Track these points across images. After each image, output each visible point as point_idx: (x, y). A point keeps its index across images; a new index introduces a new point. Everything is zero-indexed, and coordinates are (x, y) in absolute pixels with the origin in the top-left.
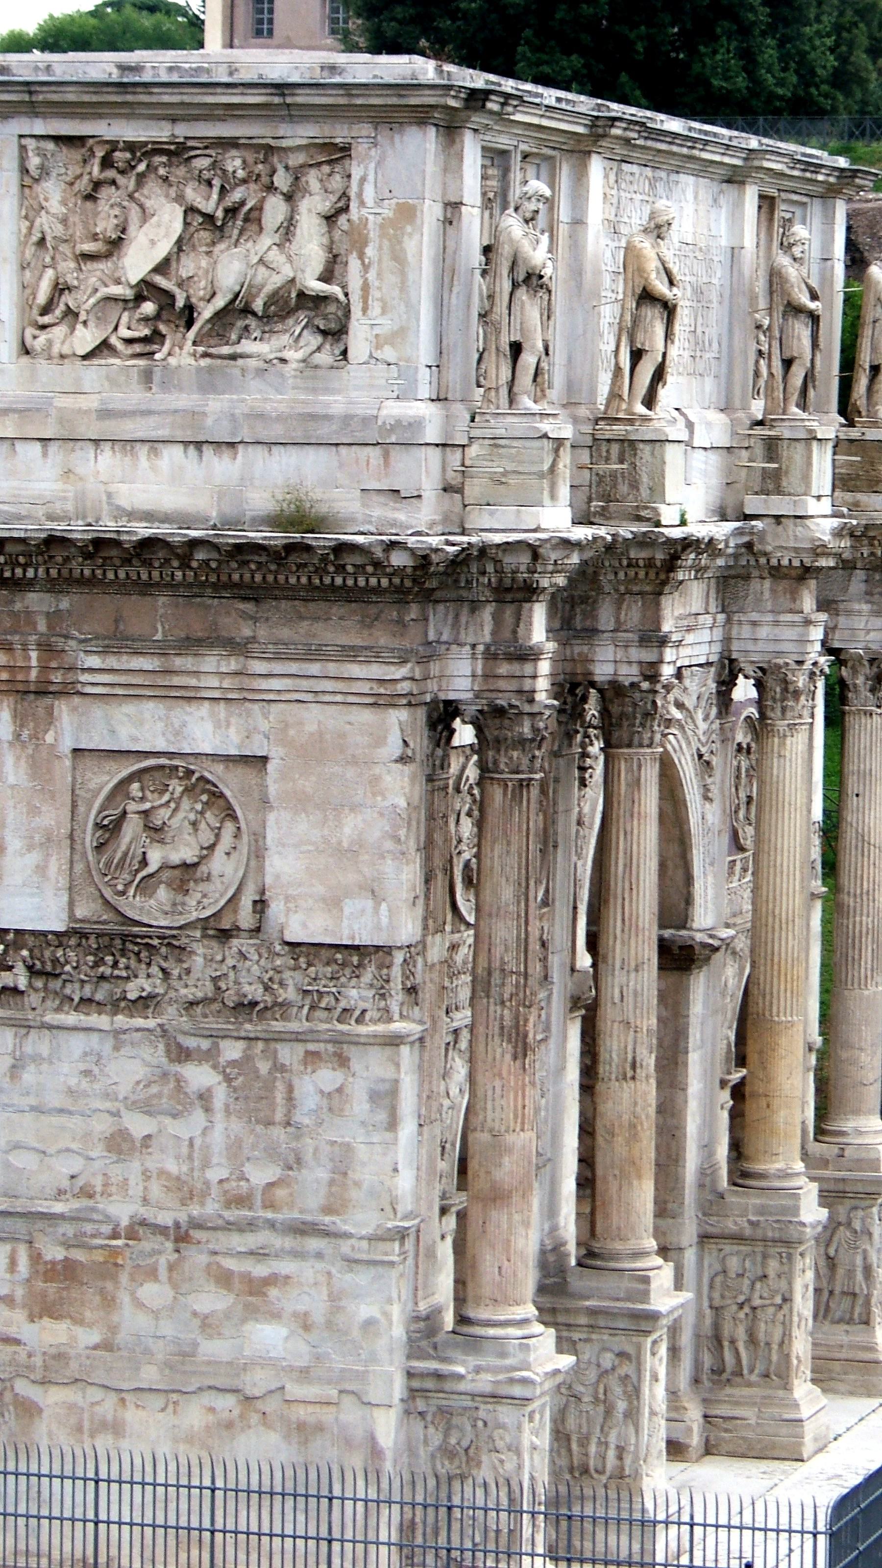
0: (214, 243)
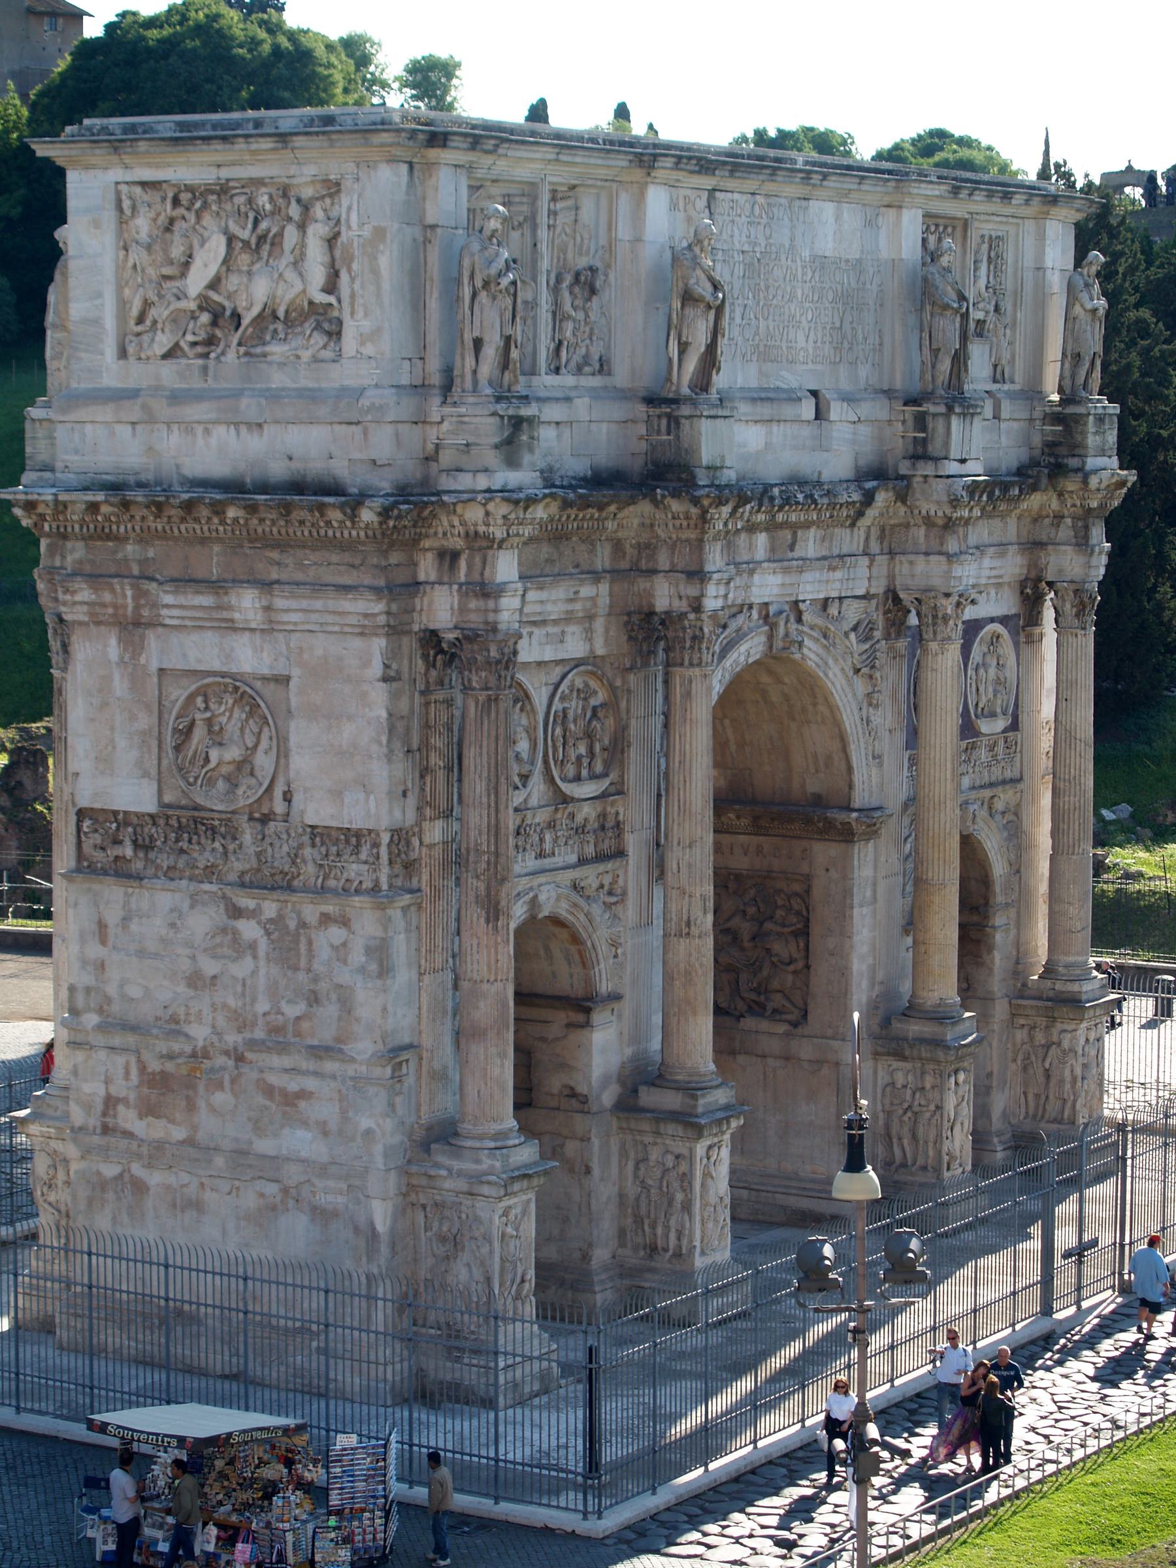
0: (253, 263)
